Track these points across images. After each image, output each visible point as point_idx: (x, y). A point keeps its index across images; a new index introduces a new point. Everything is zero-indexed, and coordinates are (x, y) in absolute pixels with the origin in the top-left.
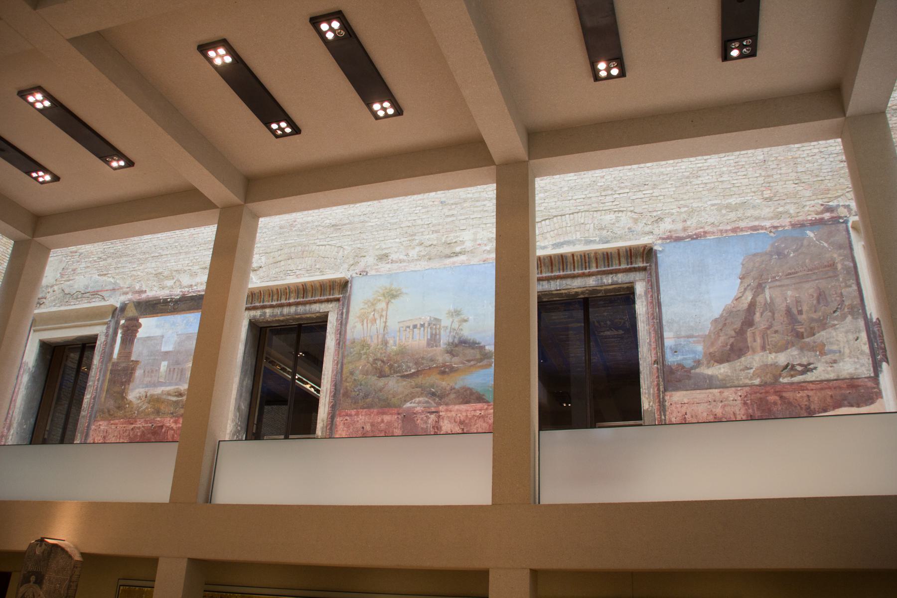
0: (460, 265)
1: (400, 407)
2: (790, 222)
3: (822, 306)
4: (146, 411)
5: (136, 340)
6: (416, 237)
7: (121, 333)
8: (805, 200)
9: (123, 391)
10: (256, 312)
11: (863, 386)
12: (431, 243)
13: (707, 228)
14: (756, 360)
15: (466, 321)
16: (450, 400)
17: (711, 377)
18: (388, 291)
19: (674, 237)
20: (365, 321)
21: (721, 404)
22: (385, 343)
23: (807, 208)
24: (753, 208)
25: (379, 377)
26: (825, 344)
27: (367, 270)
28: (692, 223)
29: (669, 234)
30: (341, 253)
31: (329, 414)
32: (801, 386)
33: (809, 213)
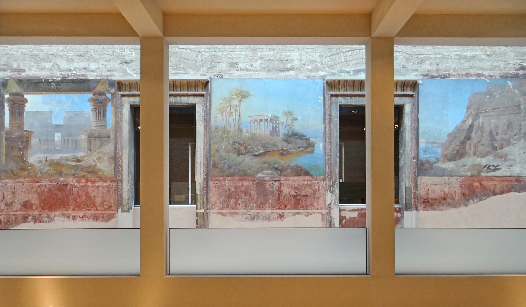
0: (291, 78)
1: (254, 176)
2: (500, 74)
3: (509, 131)
4: (49, 172)
5: (24, 113)
6: (258, 52)
7: (8, 106)
8: (510, 59)
9: (23, 156)
10: (135, 99)
11: (523, 181)
12: (269, 59)
13: (451, 72)
14: (470, 161)
15: (296, 119)
16: (287, 173)
17: (444, 169)
18: (240, 92)
19: (430, 75)
20: (224, 112)
21: (448, 186)
22: (241, 131)
23: (510, 65)
24: (479, 60)
25: (238, 155)
26: (508, 155)
27: (222, 73)
28: (442, 67)
29: (428, 72)
30: (200, 57)
31: (204, 180)
32: (491, 179)
33: (512, 69)
